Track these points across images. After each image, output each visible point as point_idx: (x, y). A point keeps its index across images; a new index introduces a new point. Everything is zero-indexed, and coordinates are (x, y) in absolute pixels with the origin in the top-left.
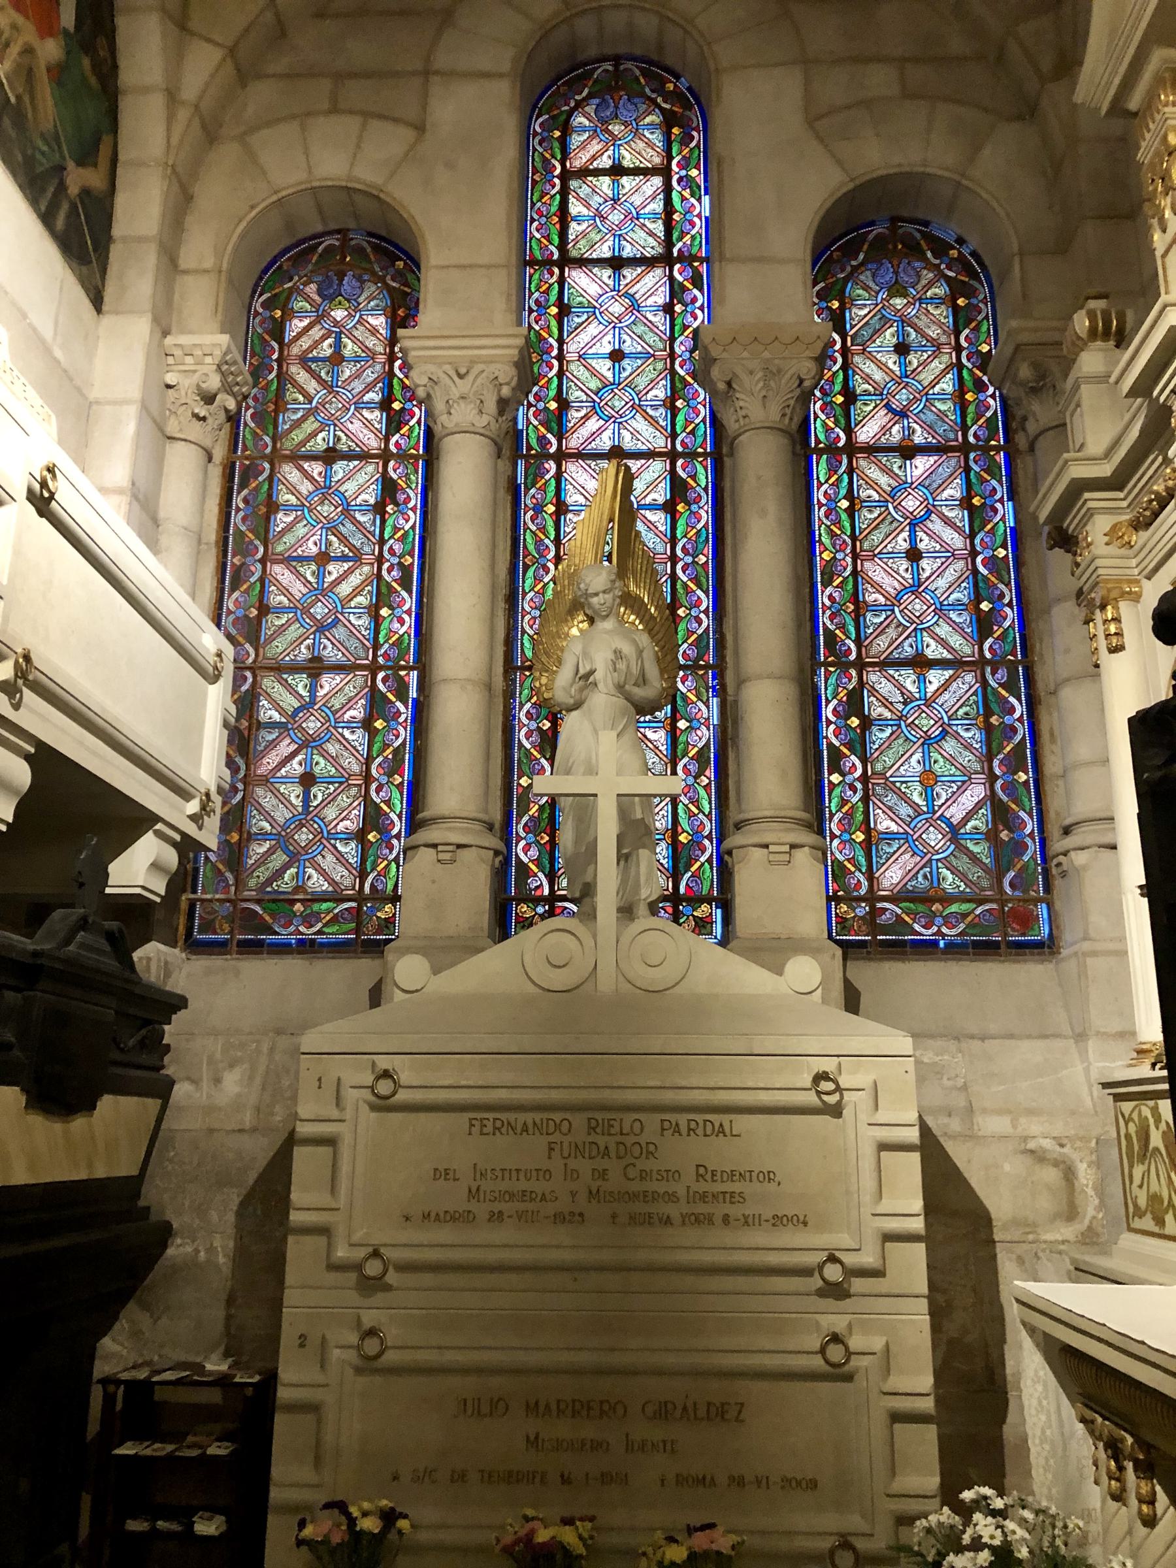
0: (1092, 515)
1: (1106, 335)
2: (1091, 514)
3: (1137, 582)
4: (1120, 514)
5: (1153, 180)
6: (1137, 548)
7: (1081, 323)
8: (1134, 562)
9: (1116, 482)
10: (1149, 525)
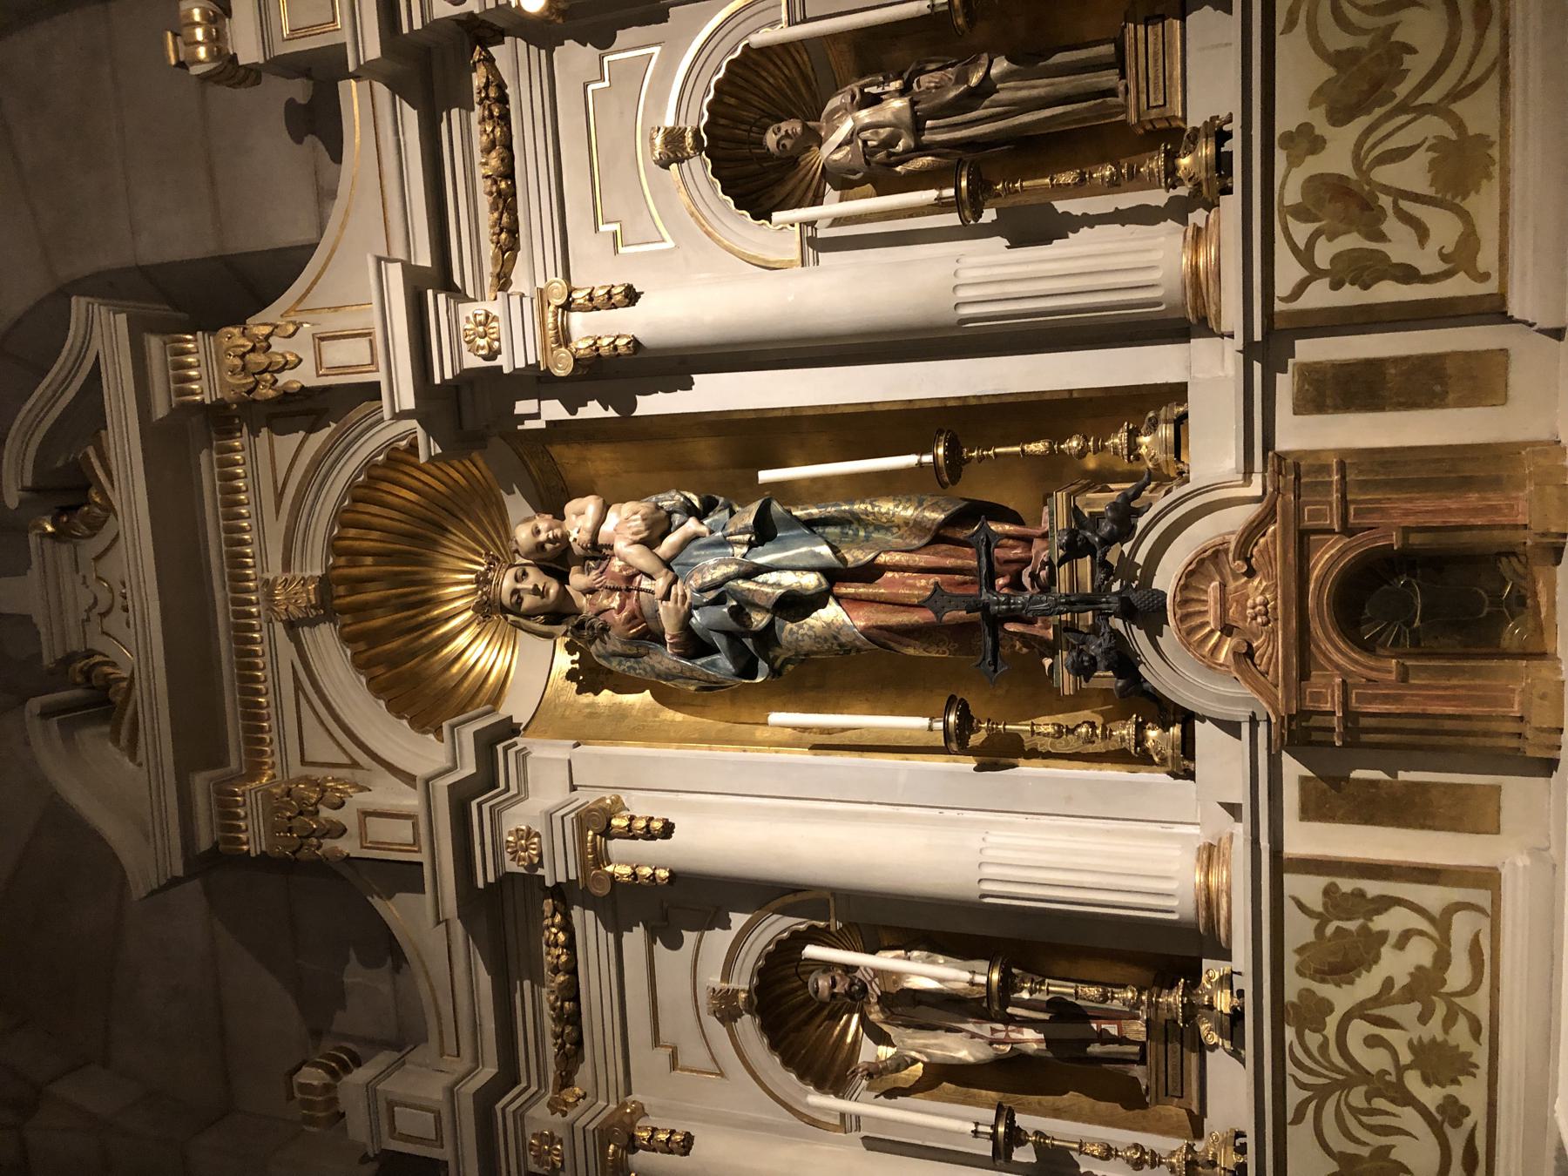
0: (522, 1117)
1: (348, 1070)
2: (519, 1115)
3: (625, 1105)
4: (540, 1098)
5: (290, 830)
6: (589, 1088)
7: (312, 1076)
8: (602, 1103)
9: (508, 1076)
10: (579, 1043)
